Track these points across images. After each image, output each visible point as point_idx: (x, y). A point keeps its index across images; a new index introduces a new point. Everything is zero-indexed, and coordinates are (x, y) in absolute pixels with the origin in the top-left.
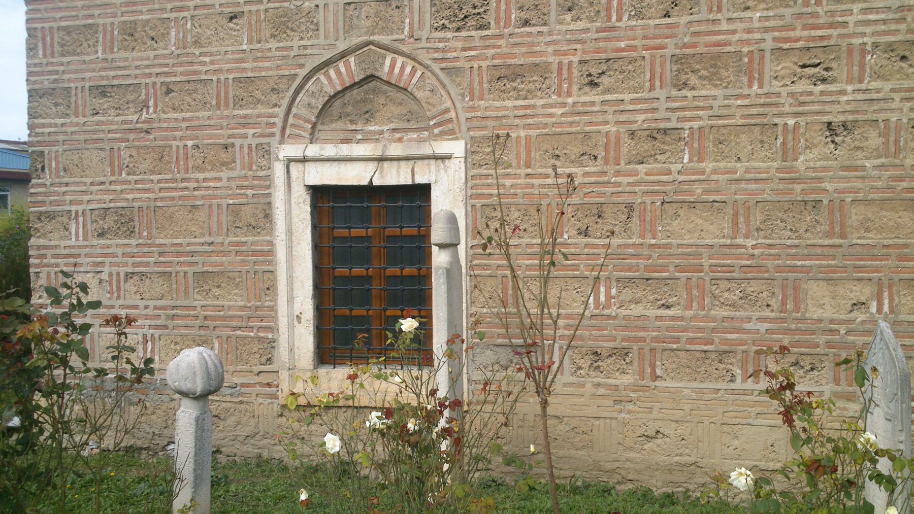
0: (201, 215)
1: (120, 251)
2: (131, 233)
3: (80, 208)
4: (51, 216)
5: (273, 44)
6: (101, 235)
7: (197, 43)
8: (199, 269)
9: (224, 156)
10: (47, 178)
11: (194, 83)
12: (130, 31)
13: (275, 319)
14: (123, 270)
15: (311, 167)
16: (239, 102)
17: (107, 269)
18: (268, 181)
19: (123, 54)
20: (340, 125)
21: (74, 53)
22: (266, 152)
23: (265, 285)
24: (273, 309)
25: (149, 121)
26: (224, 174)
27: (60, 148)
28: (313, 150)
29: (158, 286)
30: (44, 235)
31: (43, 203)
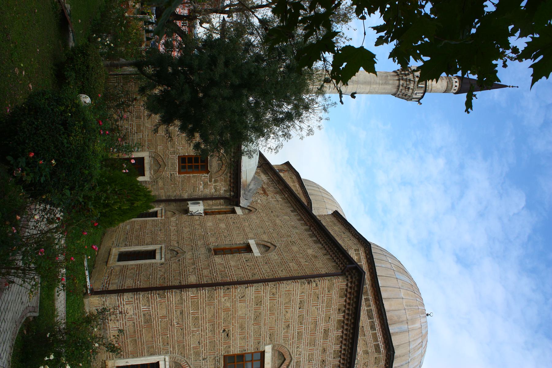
0: (150, 339)
1: (140, 320)
2: (145, 323)
3: (151, 309)
4: (148, 301)
5: (192, 352)
6: (144, 315)
7: (193, 335)
8: (137, 340)
9: (165, 344)
10: (158, 299)
11: (183, 335)
12: (197, 318)
13: (127, 358)
14: (135, 321)
15: (164, 362)
16: (179, 346)
17: (135, 317)
18: (160, 354)
19: (191, 318)
20: (174, 365)
21: (192, 305)
22: (167, 353)
23: (135, 355)
24: (129, 358)
25: (174, 325)
26: (161, 344)
27: (166, 303)
28: (167, 363)
29: (132, 330)
30: (143, 299)
31: (151, 299)
